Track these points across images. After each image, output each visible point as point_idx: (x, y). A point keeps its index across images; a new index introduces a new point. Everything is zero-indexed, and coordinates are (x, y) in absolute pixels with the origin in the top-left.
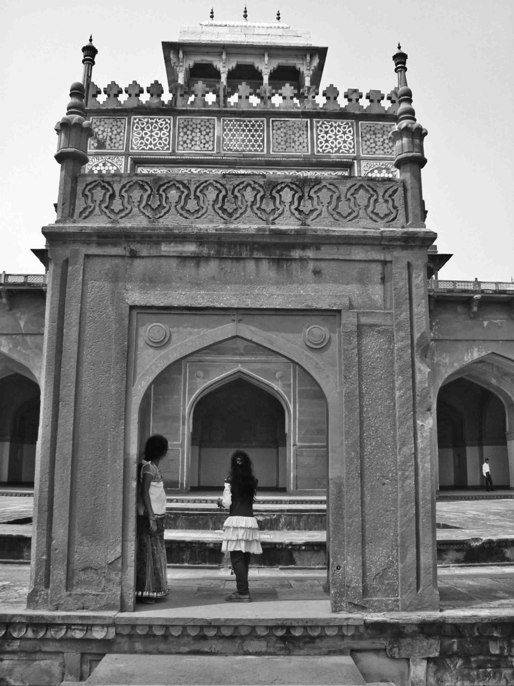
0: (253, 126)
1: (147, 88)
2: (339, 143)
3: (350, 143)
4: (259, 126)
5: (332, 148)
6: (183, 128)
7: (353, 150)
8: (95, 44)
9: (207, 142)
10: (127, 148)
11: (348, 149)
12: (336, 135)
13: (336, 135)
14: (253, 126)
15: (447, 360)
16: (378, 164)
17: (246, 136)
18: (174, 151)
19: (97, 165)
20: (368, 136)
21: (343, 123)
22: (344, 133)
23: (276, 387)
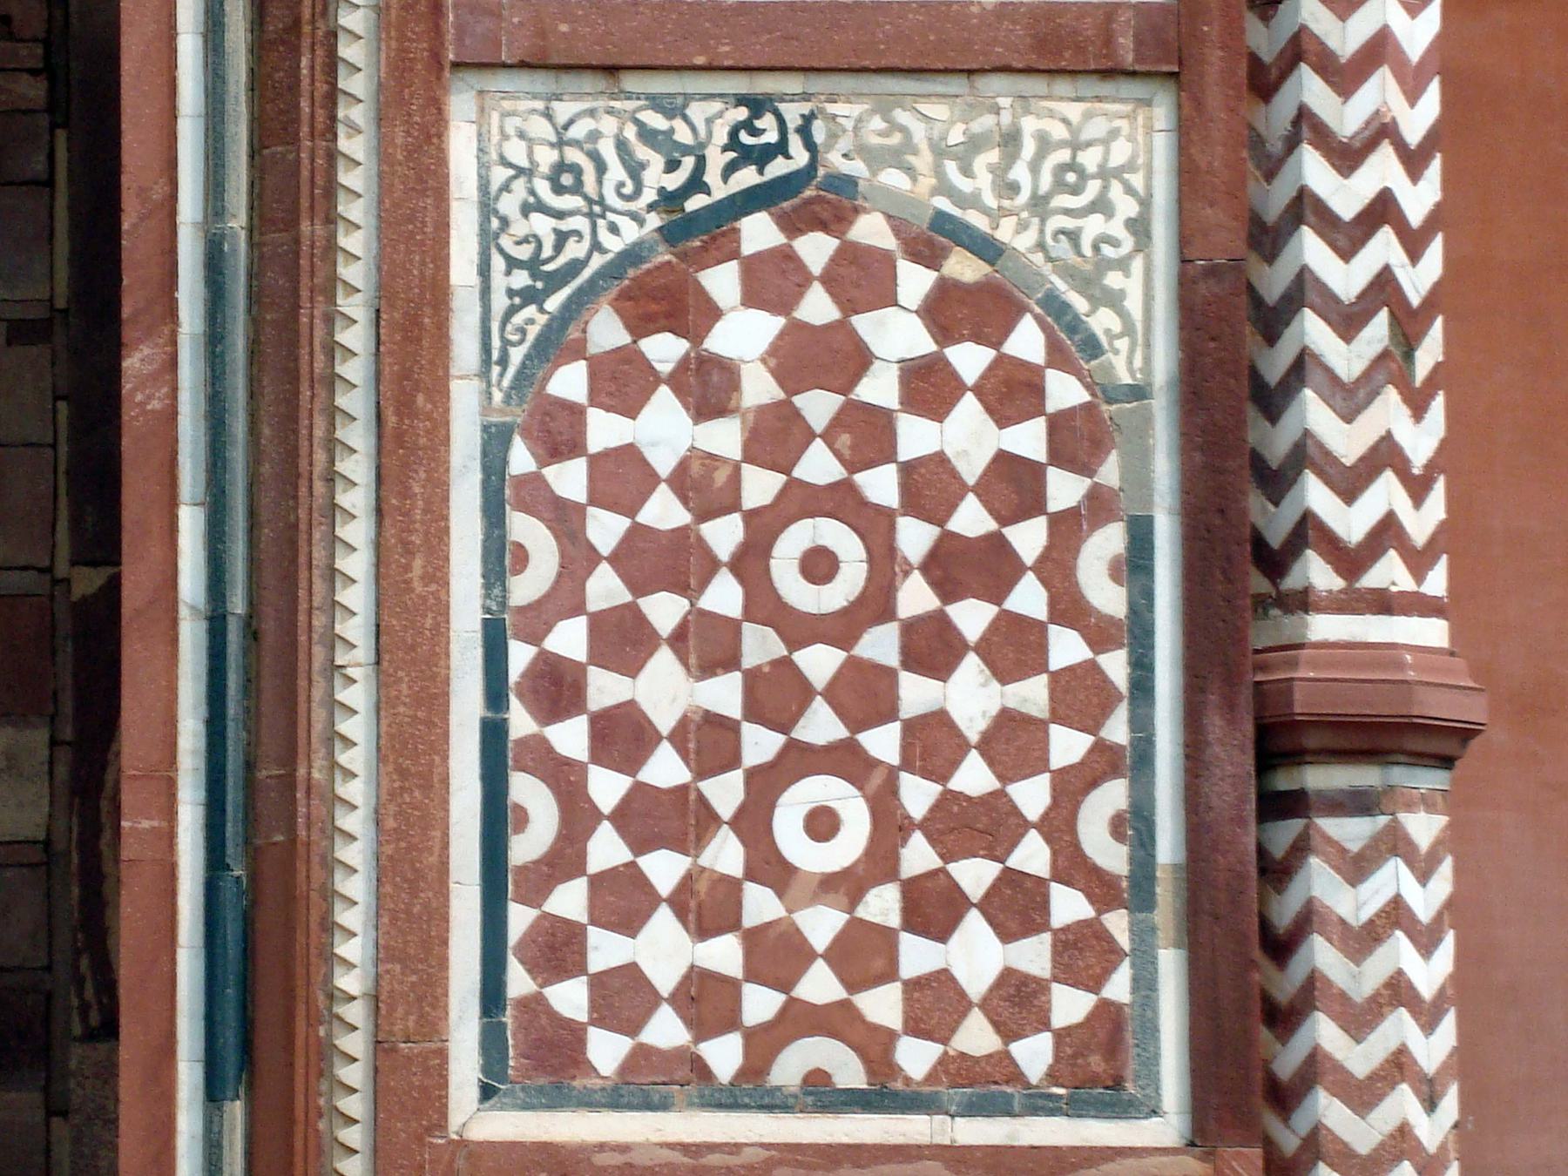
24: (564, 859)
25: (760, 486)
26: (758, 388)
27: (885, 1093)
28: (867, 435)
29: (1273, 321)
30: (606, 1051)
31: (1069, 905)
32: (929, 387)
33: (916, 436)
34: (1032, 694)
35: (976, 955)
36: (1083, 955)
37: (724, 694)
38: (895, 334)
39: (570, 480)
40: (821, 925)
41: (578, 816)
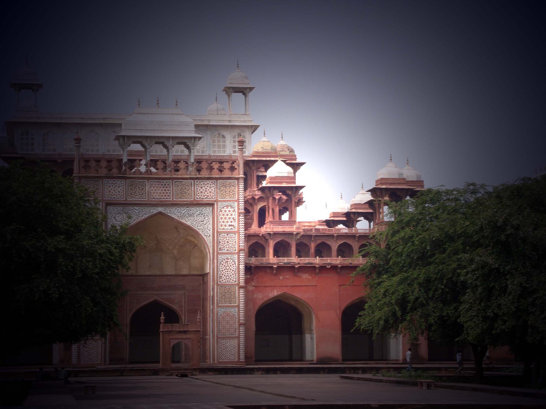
0: (165, 185)
4: (168, 185)
5: (204, 196)
9: (143, 194)
10: (102, 198)
14: (165, 185)
15: (261, 297)
16: (227, 203)
17: (162, 190)
18: (126, 198)
20: (222, 188)
21: (209, 182)
22: (210, 188)
23: (175, 307)
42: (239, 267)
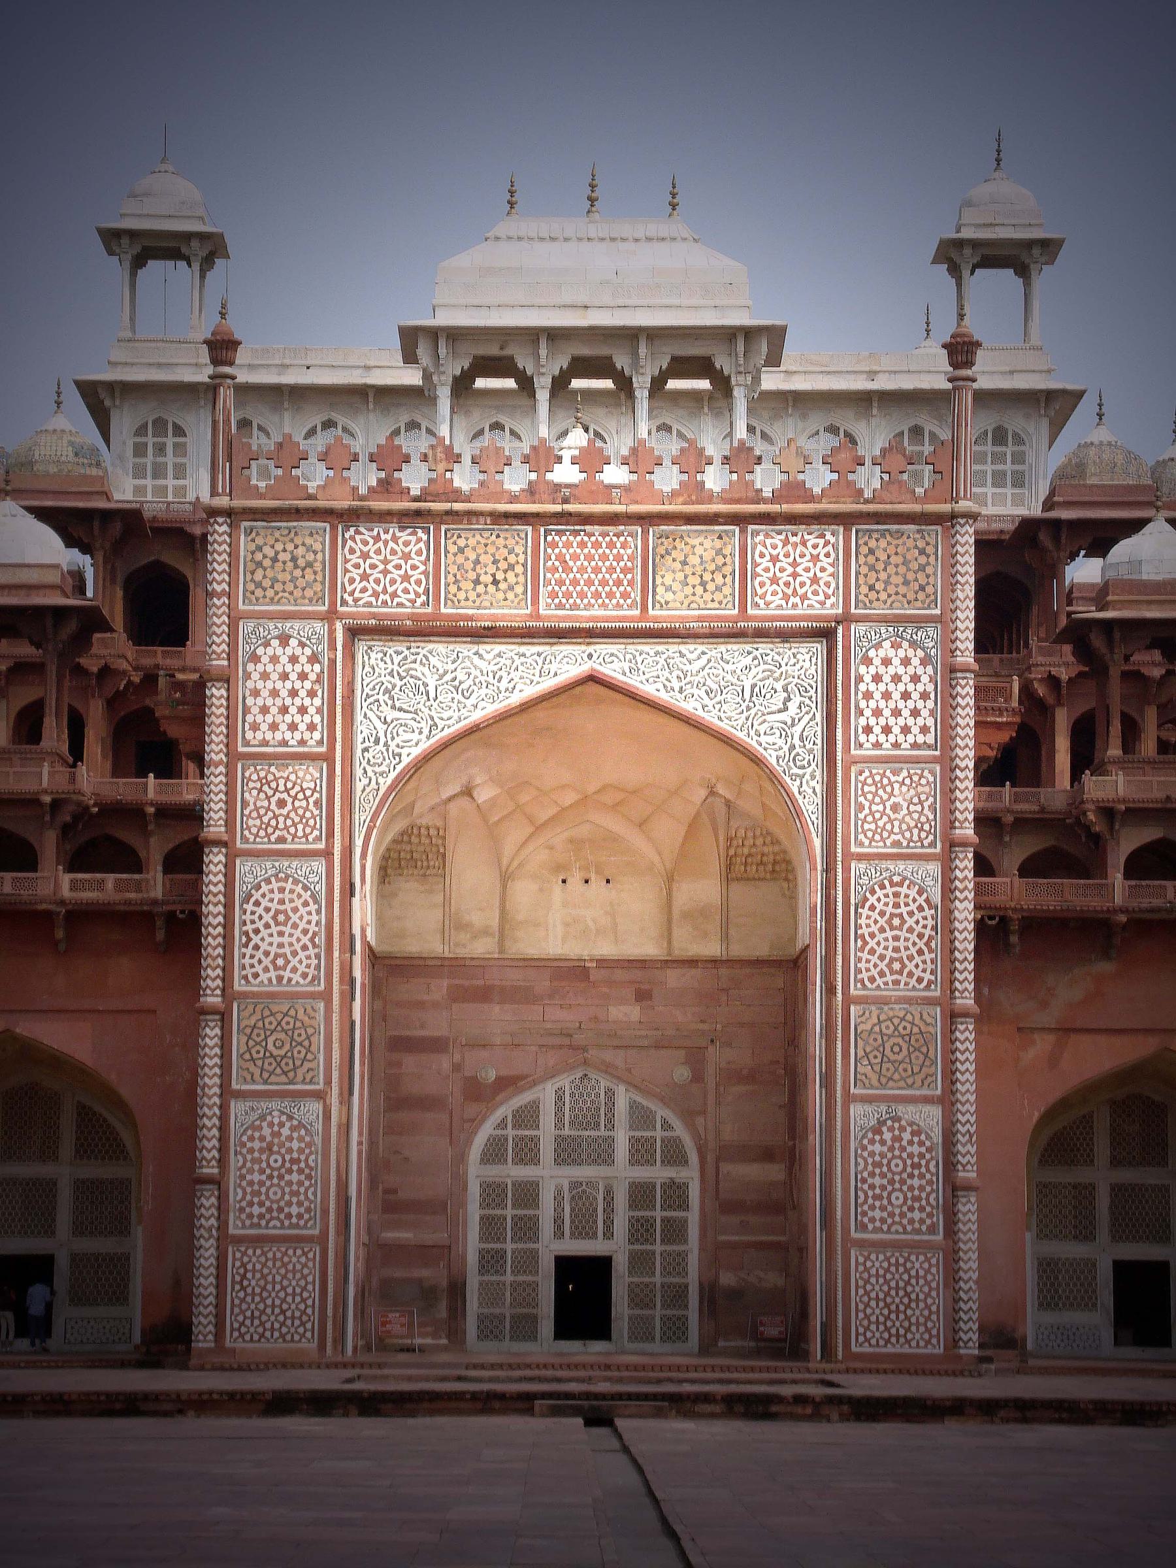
1: (371, 455)
2: (802, 584)
3: (828, 585)
4: (624, 546)
6: (455, 555)
7: (833, 599)
8: (237, 328)
10: (333, 603)
11: (821, 597)
12: (795, 564)
13: (795, 564)
19: (267, 644)
24: (866, 1201)
25: (889, 1155)
26: (889, 1143)
27: (905, 1232)
28: (903, 1149)
29: (954, 1135)
30: (870, 1226)
31: (928, 1209)
32: (911, 1143)
33: (909, 1149)
34: (924, 1182)
35: (917, 1215)
36: (930, 1215)
37: (885, 1182)
38: (906, 1136)
39: (865, 1154)
40: (897, 1211)
41: (866, 1196)
42: (948, 915)
